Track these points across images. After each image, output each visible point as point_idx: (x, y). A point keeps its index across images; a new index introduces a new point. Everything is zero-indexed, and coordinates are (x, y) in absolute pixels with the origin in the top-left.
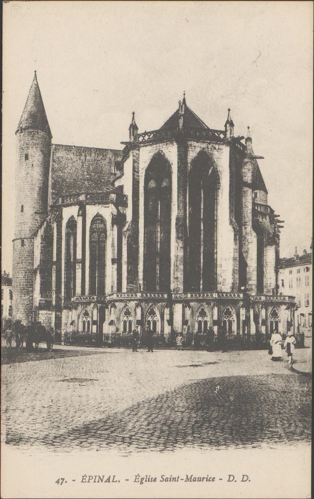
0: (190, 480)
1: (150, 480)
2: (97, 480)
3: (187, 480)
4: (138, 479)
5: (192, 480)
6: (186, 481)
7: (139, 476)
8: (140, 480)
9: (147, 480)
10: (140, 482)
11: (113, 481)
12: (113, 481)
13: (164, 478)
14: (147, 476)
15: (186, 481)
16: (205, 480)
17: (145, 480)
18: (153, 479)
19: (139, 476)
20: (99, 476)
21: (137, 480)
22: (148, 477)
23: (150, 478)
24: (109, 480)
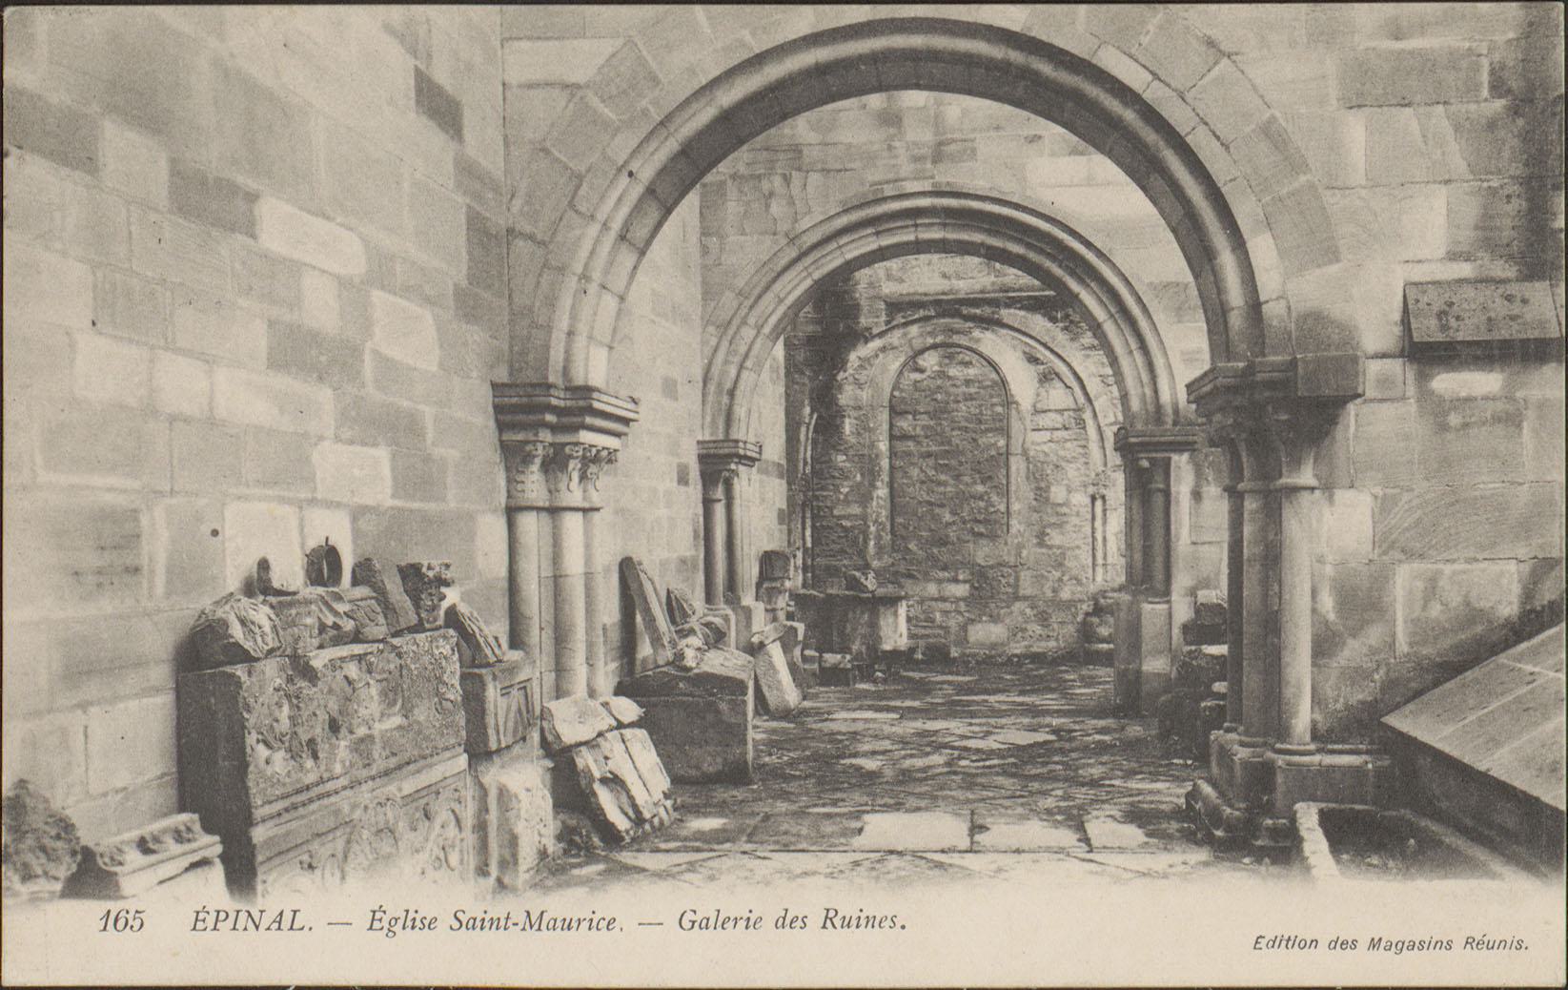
0: (536, 927)
1: (418, 923)
2: (240, 925)
3: (527, 926)
4: (380, 920)
5: (544, 927)
6: (524, 929)
7: (385, 912)
8: (387, 926)
9: (409, 923)
10: (385, 931)
11: (291, 928)
12: (291, 928)
13: (464, 918)
14: (407, 911)
15: (524, 929)
16: (585, 925)
17: (401, 922)
18: (426, 922)
19: (385, 912)
20: (248, 912)
21: (377, 925)
22: (411, 915)
23: (418, 917)
24: (280, 923)
